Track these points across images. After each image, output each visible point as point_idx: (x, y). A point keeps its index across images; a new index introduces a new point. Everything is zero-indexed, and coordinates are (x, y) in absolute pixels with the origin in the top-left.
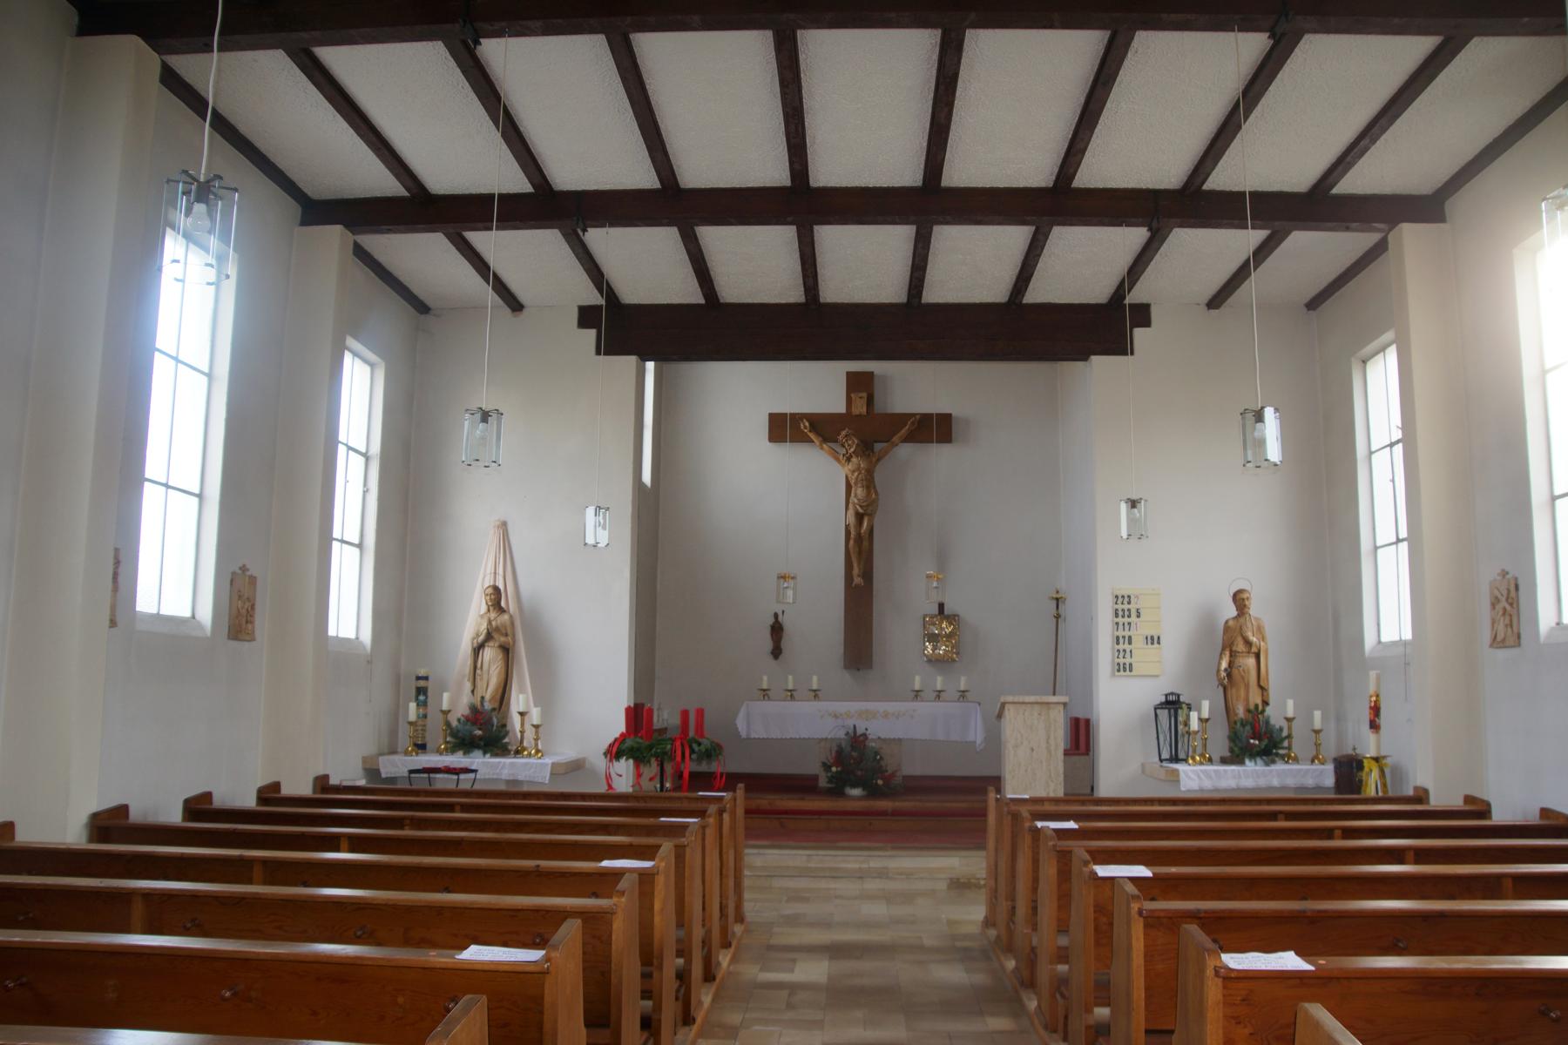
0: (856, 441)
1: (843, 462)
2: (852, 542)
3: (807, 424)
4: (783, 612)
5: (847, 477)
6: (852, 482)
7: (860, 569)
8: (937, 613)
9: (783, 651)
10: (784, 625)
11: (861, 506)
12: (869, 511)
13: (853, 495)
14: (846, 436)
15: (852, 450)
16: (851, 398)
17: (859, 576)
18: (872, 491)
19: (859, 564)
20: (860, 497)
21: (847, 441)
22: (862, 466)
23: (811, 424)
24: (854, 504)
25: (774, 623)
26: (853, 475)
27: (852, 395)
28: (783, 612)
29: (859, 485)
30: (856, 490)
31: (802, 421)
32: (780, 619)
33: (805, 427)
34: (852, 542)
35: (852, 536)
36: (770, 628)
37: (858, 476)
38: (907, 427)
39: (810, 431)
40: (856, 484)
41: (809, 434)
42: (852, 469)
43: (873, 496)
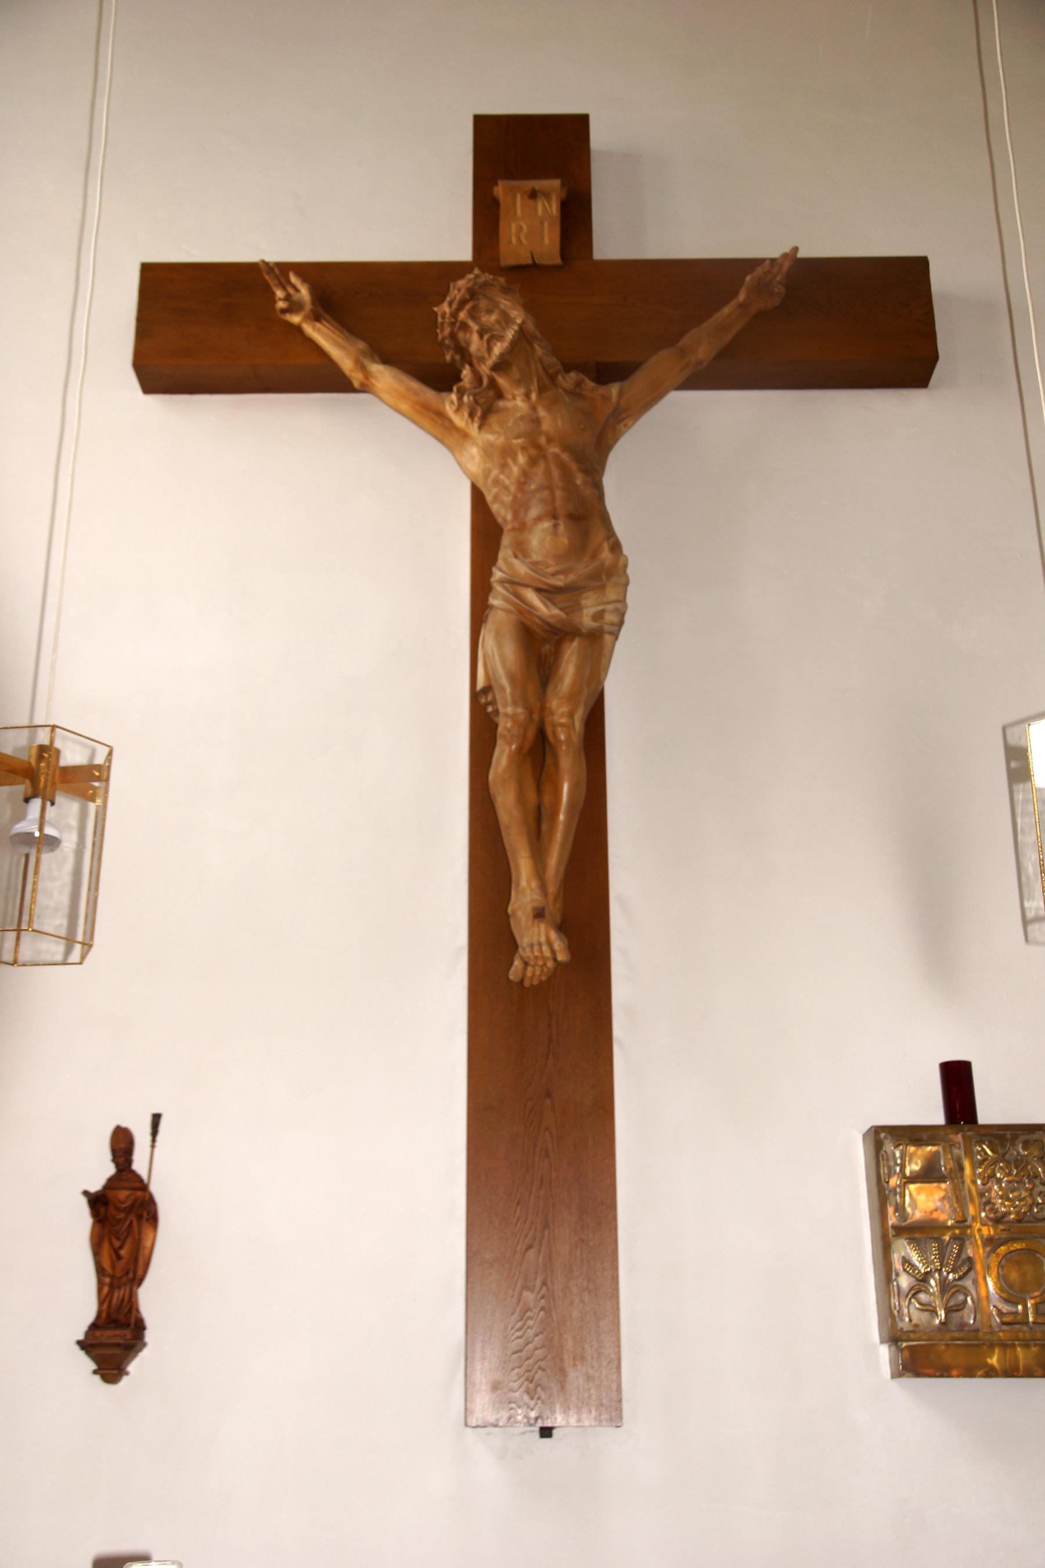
0: (518, 316)
1: (460, 420)
2: (502, 757)
3: (304, 293)
4: (156, 1119)
5: (478, 498)
6: (501, 511)
7: (543, 887)
8: (935, 1115)
9: (149, 1336)
10: (156, 1189)
11: (546, 592)
12: (586, 620)
13: (505, 553)
14: (472, 294)
15: (498, 349)
16: (496, 203)
17: (539, 914)
18: (598, 535)
19: (539, 854)
20: (535, 557)
21: (473, 315)
22: (546, 426)
23: (314, 291)
24: (513, 583)
25: (112, 1183)
26: (504, 466)
27: (500, 190)
28: (156, 1119)
29: (534, 512)
30: (522, 527)
31: (285, 284)
32: (139, 1164)
33: (294, 307)
34: (502, 757)
35: (504, 725)
36: (83, 1221)
37: (526, 475)
38: (742, 297)
39: (317, 318)
40: (519, 507)
41: (309, 329)
42: (501, 440)
43: (606, 555)
